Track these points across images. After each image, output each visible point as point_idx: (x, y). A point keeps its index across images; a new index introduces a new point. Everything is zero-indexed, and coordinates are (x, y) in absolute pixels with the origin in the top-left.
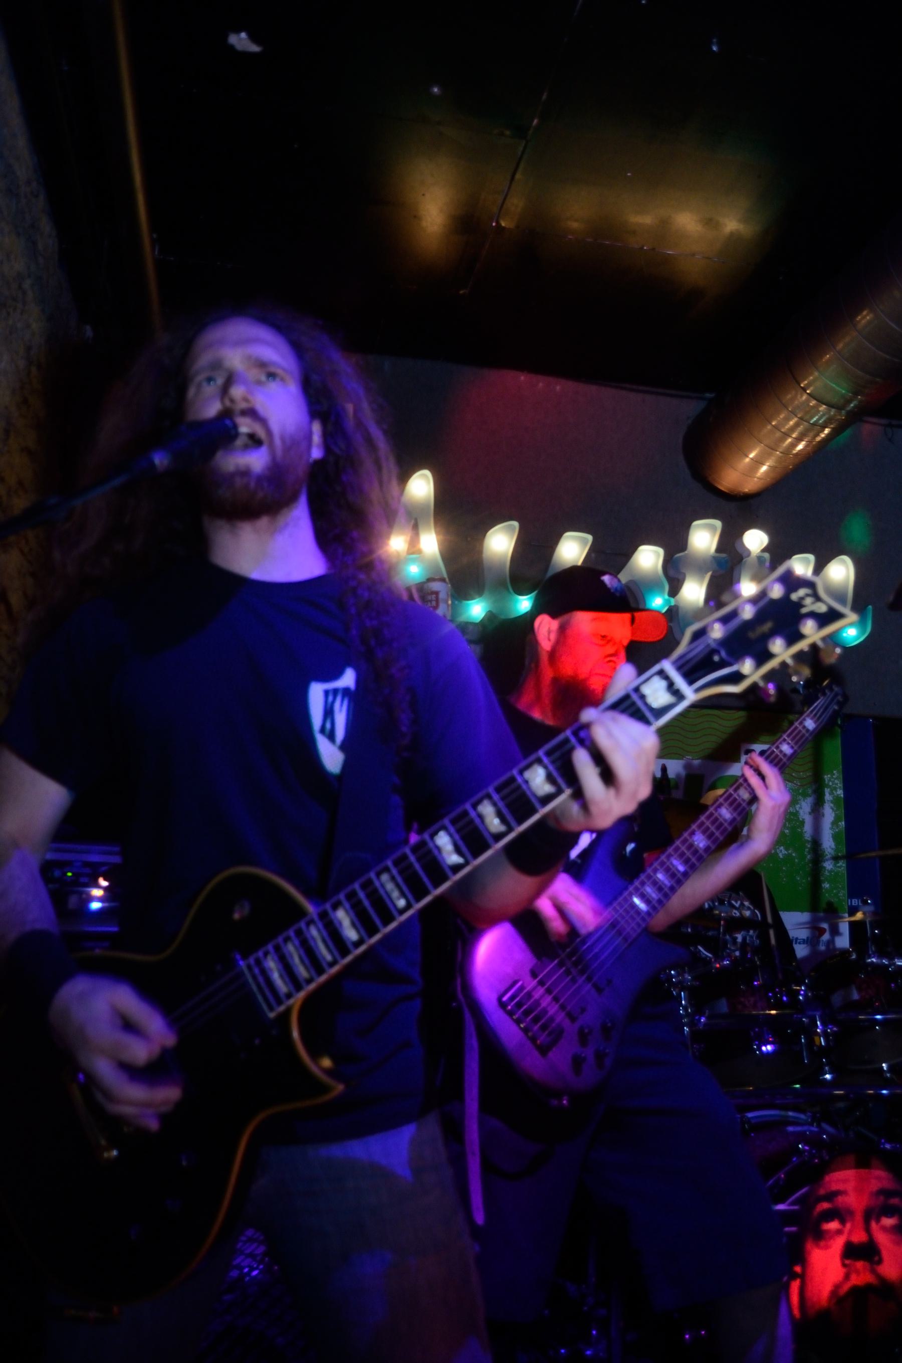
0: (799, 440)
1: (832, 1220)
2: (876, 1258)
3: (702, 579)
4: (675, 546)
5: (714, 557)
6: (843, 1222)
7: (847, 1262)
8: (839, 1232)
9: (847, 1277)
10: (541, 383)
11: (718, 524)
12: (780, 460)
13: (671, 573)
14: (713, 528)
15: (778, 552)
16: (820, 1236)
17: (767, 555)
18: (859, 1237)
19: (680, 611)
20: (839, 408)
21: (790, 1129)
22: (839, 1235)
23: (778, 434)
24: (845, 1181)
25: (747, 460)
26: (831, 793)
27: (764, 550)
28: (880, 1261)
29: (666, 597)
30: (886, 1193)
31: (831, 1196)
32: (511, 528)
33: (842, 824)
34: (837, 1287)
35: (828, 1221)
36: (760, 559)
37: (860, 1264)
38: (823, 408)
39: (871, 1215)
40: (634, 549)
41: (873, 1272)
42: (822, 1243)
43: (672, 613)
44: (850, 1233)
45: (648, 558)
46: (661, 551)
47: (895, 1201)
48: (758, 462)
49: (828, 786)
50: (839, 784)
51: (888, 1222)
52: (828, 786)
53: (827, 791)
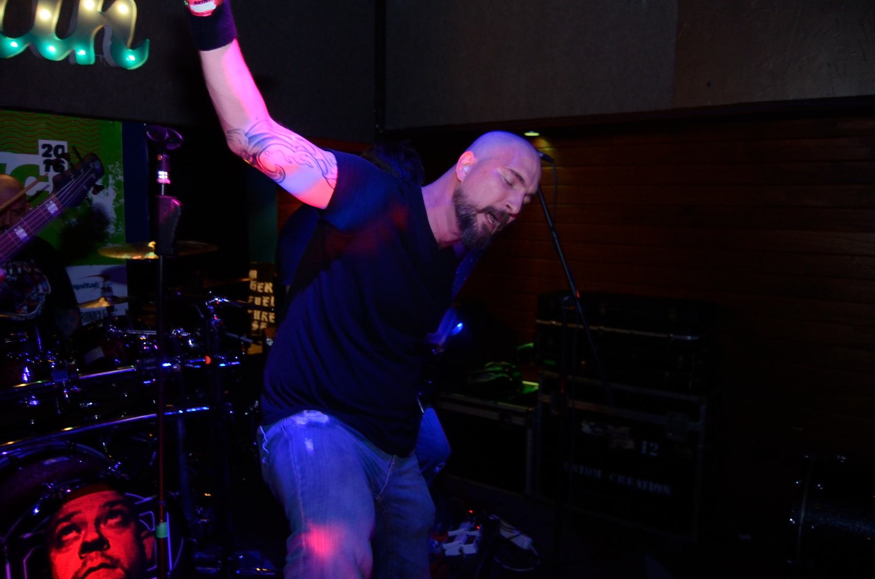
1: (71, 532)
2: (105, 547)
6: (79, 531)
7: (83, 555)
8: (76, 538)
9: (84, 564)
16: (60, 545)
18: (92, 536)
22: (75, 541)
26: (114, 178)
28: (109, 547)
30: (111, 504)
31: (68, 518)
33: (123, 200)
34: (77, 573)
35: (67, 534)
37: (93, 554)
39: (98, 522)
41: (103, 555)
42: (64, 549)
44: (86, 535)
47: (118, 507)
49: (111, 173)
50: (120, 171)
51: (112, 522)
52: (111, 173)
53: (110, 177)
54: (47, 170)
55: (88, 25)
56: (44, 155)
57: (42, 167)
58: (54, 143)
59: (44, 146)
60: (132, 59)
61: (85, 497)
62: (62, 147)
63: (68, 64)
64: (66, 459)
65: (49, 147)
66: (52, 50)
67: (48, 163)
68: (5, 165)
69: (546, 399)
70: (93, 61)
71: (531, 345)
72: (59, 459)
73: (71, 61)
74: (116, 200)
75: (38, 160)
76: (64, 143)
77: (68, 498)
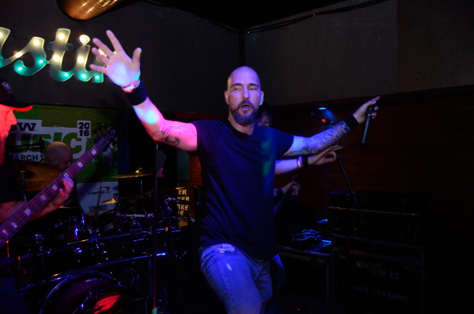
3: (62, 53)
5: (67, 45)
11: (69, 31)
12: (94, 10)
13: (48, 49)
14: (66, 32)
17: (89, 46)
21: (87, 281)
24: (104, 302)
25: (81, 7)
29: (45, 60)
36: (86, 47)
40: (31, 38)
43: (48, 67)
45: (37, 42)
46: (43, 40)
48: (86, 9)
54: (81, 135)
56: (80, 128)
57: (79, 134)
58: (84, 122)
59: (80, 124)
61: (107, 298)
62: (88, 123)
63: (91, 82)
64: (96, 279)
65: (82, 123)
66: (84, 77)
67: (81, 132)
68: (61, 133)
69: (336, 249)
70: (102, 81)
71: (327, 220)
72: (93, 280)
73: (93, 82)
75: (76, 130)
76: (89, 122)
77: (100, 298)
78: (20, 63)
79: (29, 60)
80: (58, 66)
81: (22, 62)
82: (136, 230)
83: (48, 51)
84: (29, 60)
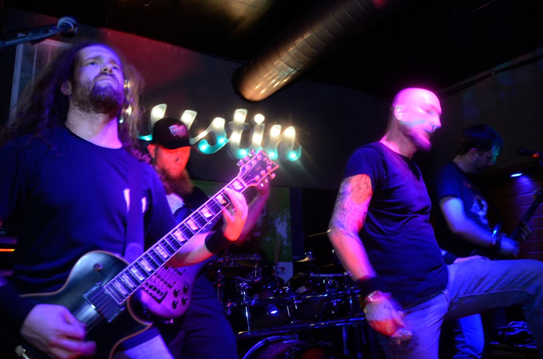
0: (278, 80)
3: (239, 132)
4: (229, 118)
10: (176, 49)
11: (245, 111)
14: (243, 113)
15: (268, 123)
17: (264, 125)
19: (231, 145)
20: (295, 69)
21: (285, 342)
23: (270, 78)
25: (258, 87)
27: (263, 122)
29: (225, 138)
32: (163, 107)
33: (290, 228)
36: (261, 127)
38: (289, 69)
43: (227, 146)
45: (218, 123)
48: (261, 88)
53: (284, 216)
55: (276, 141)
60: (294, 156)
74: (287, 228)
78: (204, 142)
79: (212, 139)
80: (236, 145)
81: (205, 141)
82: (332, 290)
83: (228, 130)
84: (212, 139)
